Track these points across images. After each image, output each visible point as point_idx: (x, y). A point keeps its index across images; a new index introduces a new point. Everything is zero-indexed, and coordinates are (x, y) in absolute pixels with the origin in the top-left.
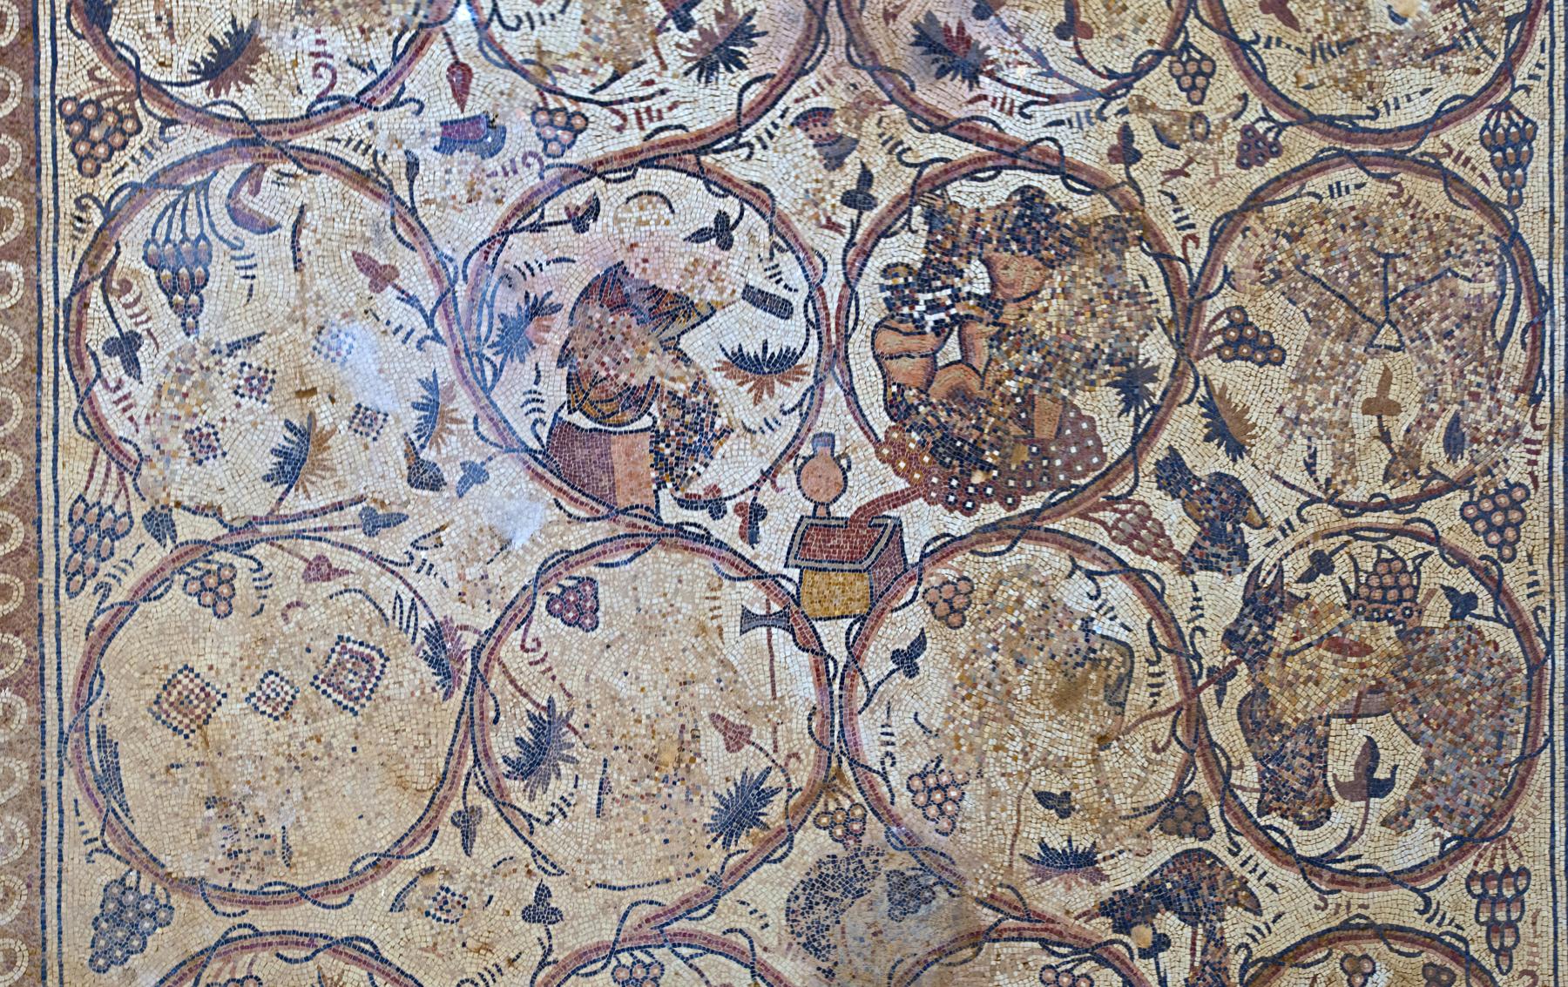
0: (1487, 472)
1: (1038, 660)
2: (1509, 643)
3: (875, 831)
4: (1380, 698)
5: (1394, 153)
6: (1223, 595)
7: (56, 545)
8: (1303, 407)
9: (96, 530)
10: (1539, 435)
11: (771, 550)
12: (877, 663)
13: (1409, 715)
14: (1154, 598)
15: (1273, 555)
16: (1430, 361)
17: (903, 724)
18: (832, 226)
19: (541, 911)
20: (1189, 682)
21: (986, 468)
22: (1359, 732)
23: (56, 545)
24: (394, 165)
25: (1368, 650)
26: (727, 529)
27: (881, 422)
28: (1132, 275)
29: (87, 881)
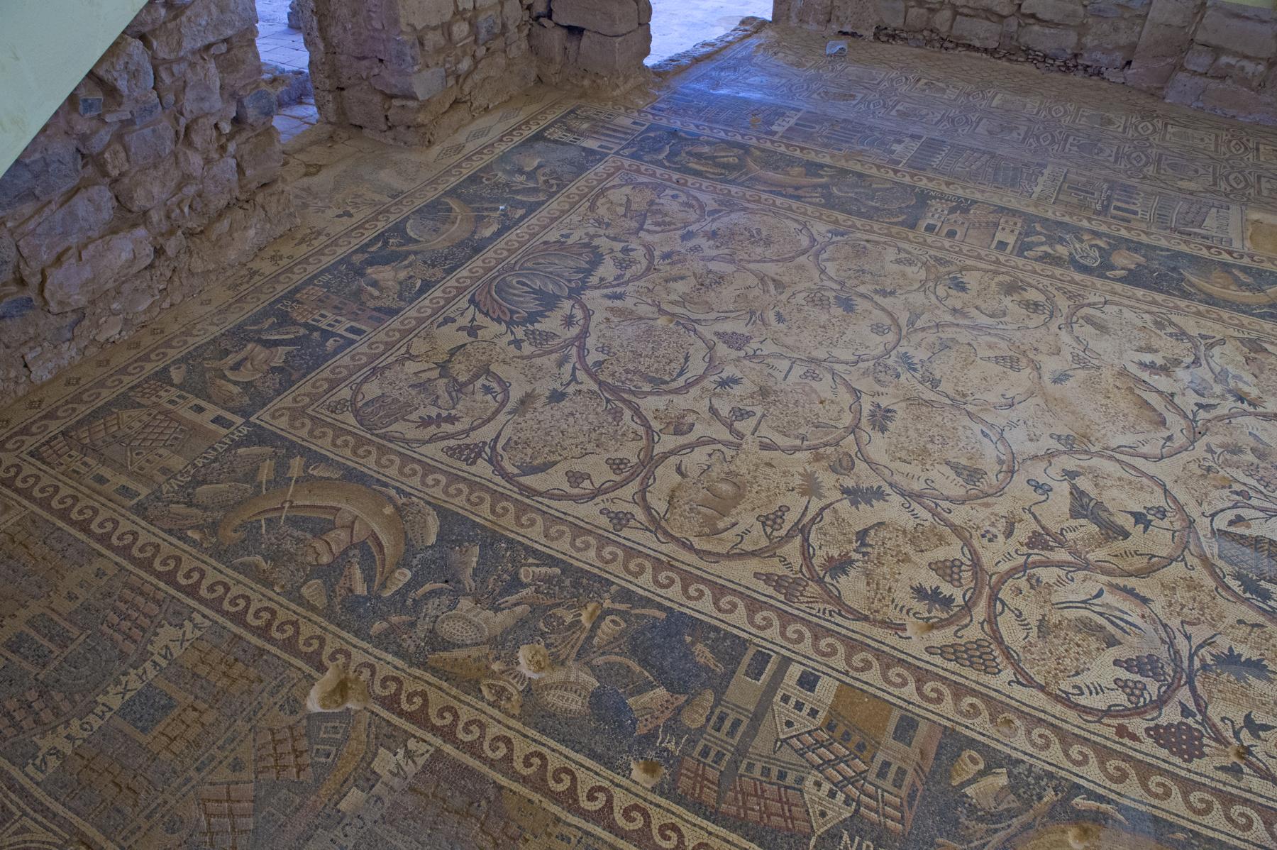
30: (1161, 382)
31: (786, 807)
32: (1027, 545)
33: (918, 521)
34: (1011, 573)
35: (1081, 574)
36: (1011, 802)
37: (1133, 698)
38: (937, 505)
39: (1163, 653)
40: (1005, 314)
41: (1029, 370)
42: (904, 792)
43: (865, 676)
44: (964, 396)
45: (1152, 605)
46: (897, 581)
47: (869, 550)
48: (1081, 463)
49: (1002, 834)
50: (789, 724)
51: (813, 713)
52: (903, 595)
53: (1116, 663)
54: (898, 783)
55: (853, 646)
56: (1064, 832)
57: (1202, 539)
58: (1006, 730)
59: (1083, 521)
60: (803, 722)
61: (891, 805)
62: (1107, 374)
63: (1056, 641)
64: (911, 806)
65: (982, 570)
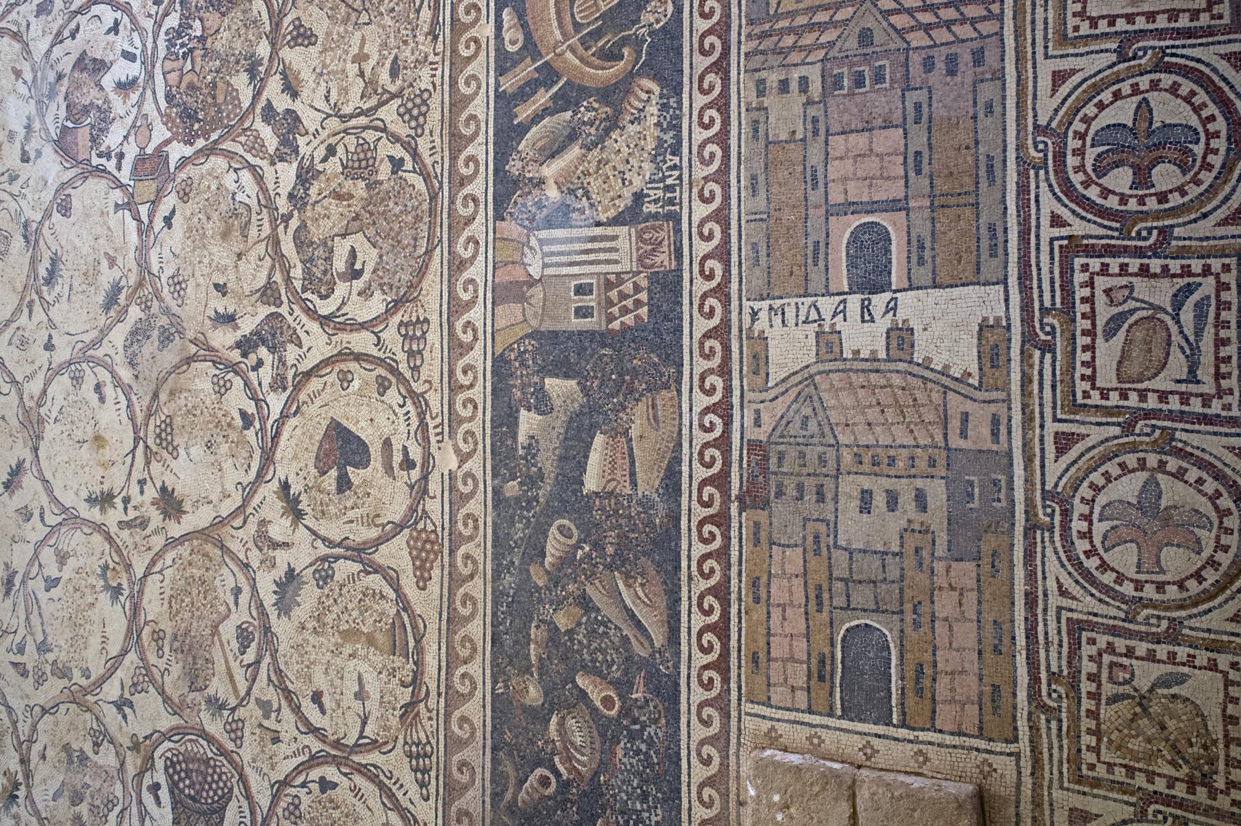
0: (411, 85)
1: (215, 216)
3: (155, 308)
4: (357, 224)
8: (324, 66)
10: (437, 59)
11: (125, 176)
12: (158, 223)
13: (371, 232)
15: (310, 148)
16: (384, 27)
18: (150, 16)
21: (199, 121)
25: (351, 196)
26: (111, 165)
27: (163, 104)
28: (255, 12)
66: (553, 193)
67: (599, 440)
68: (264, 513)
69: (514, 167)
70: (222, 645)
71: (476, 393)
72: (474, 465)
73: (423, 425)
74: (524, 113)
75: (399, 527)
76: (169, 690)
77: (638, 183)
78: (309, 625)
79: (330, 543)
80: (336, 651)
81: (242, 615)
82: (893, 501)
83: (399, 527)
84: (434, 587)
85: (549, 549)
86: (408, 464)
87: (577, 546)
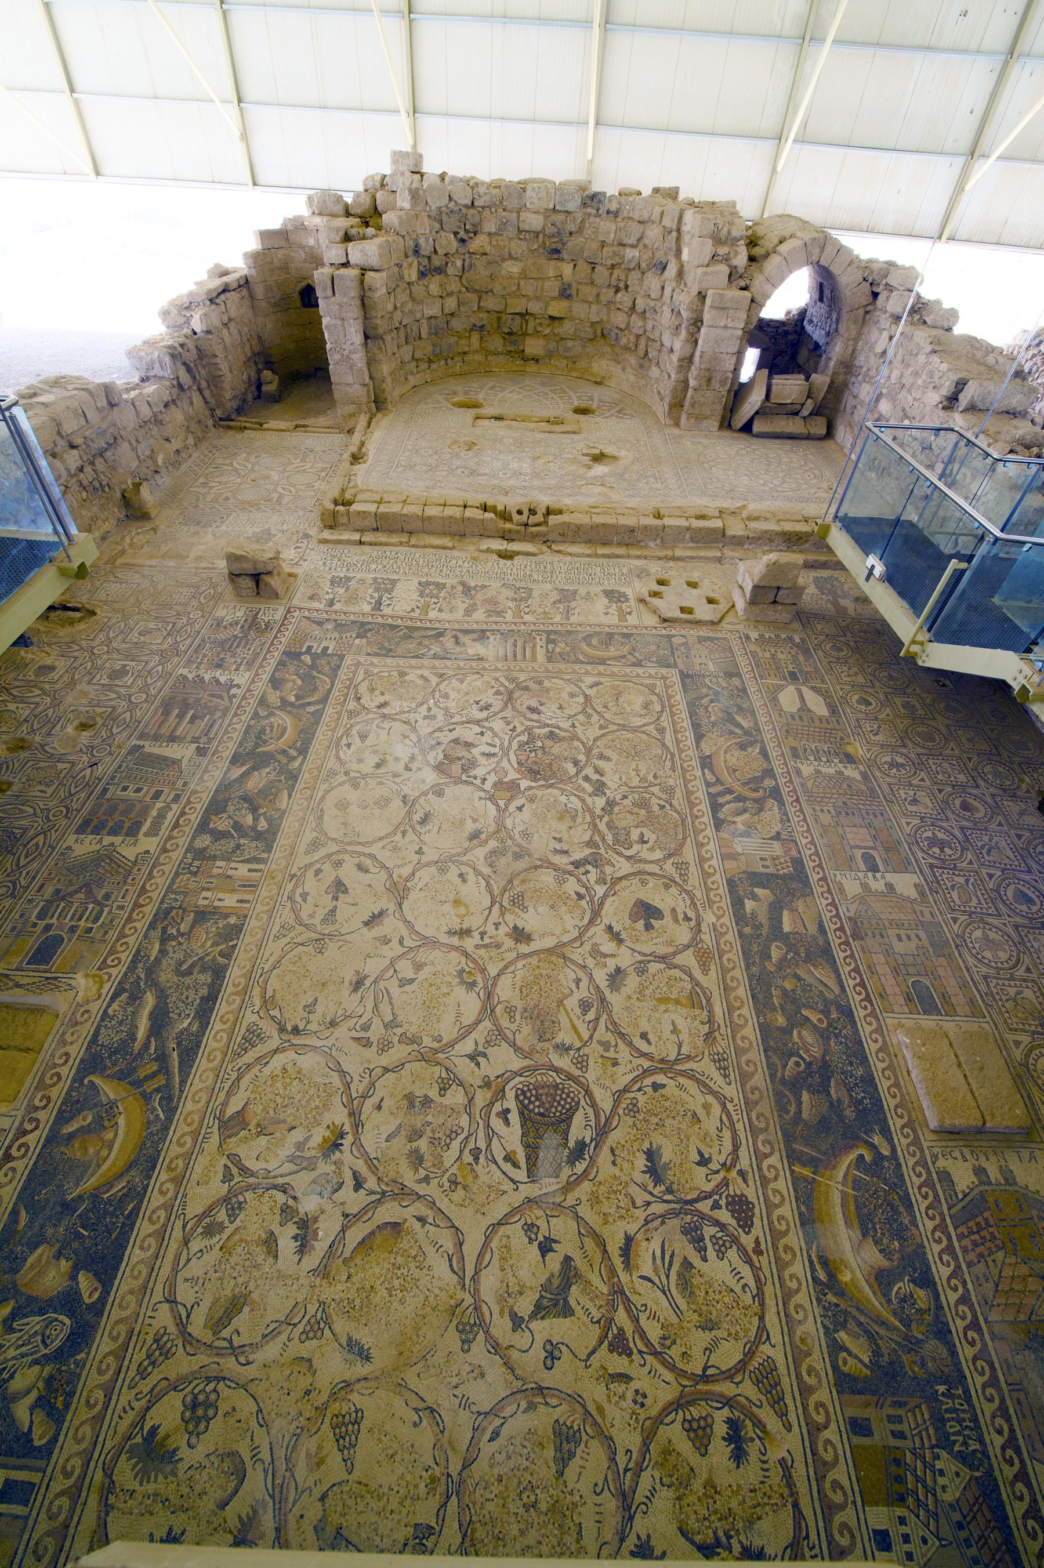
2: (675, 815)
3: (509, 842)
5: (635, 730)
6: (600, 802)
7: (323, 774)
9: (333, 773)
11: (488, 786)
12: (512, 808)
14: (583, 801)
17: (517, 821)
19: (420, 852)
20: (593, 817)
22: (638, 831)
23: (323, 774)
24: (413, 721)
27: (516, 766)
29: (309, 836)
30: (327, 1230)
31: (975, 1509)
32: (630, 1355)
33: (658, 1486)
34: (672, 1367)
35: (633, 1298)
36: (851, 1324)
37: (728, 1245)
38: (626, 1470)
39: (674, 1223)
40: (233, 1454)
41: (354, 1397)
42: (901, 1412)
43: (846, 1483)
44: (433, 1480)
45: (631, 1232)
46: (739, 1486)
47: (721, 1533)
48: (496, 1310)
49: (876, 1327)
50: (925, 1541)
51: (902, 1521)
52: (751, 1473)
53: (705, 1259)
54: (899, 1420)
55: (829, 1510)
56: (846, 1284)
57: (544, 1191)
58: (809, 1341)
59: (572, 1302)
60: (915, 1528)
61: (916, 1420)
62: (328, 1293)
63: (714, 1313)
64: (905, 1404)
65: (681, 1397)
66: (741, 827)
67: (785, 913)
68: (594, 940)
69: (721, 816)
70: (567, 1012)
71: (721, 891)
72: (725, 920)
73: (693, 902)
74: (721, 800)
75: (687, 947)
76: (519, 1043)
77: (777, 829)
78: (634, 997)
79: (644, 955)
80: (655, 1009)
81: (583, 992)
82: (909, 938)
83: (687, 947)
84: (713, 973)
85: (773, 954)
86: (687, 919)
87: (787, 954)
